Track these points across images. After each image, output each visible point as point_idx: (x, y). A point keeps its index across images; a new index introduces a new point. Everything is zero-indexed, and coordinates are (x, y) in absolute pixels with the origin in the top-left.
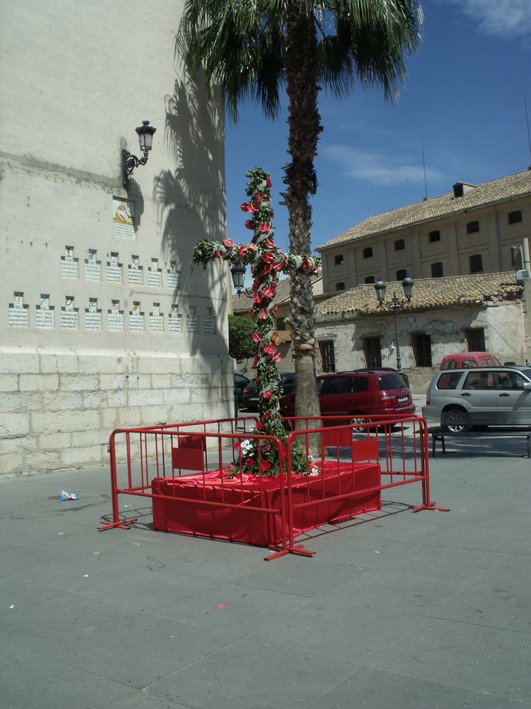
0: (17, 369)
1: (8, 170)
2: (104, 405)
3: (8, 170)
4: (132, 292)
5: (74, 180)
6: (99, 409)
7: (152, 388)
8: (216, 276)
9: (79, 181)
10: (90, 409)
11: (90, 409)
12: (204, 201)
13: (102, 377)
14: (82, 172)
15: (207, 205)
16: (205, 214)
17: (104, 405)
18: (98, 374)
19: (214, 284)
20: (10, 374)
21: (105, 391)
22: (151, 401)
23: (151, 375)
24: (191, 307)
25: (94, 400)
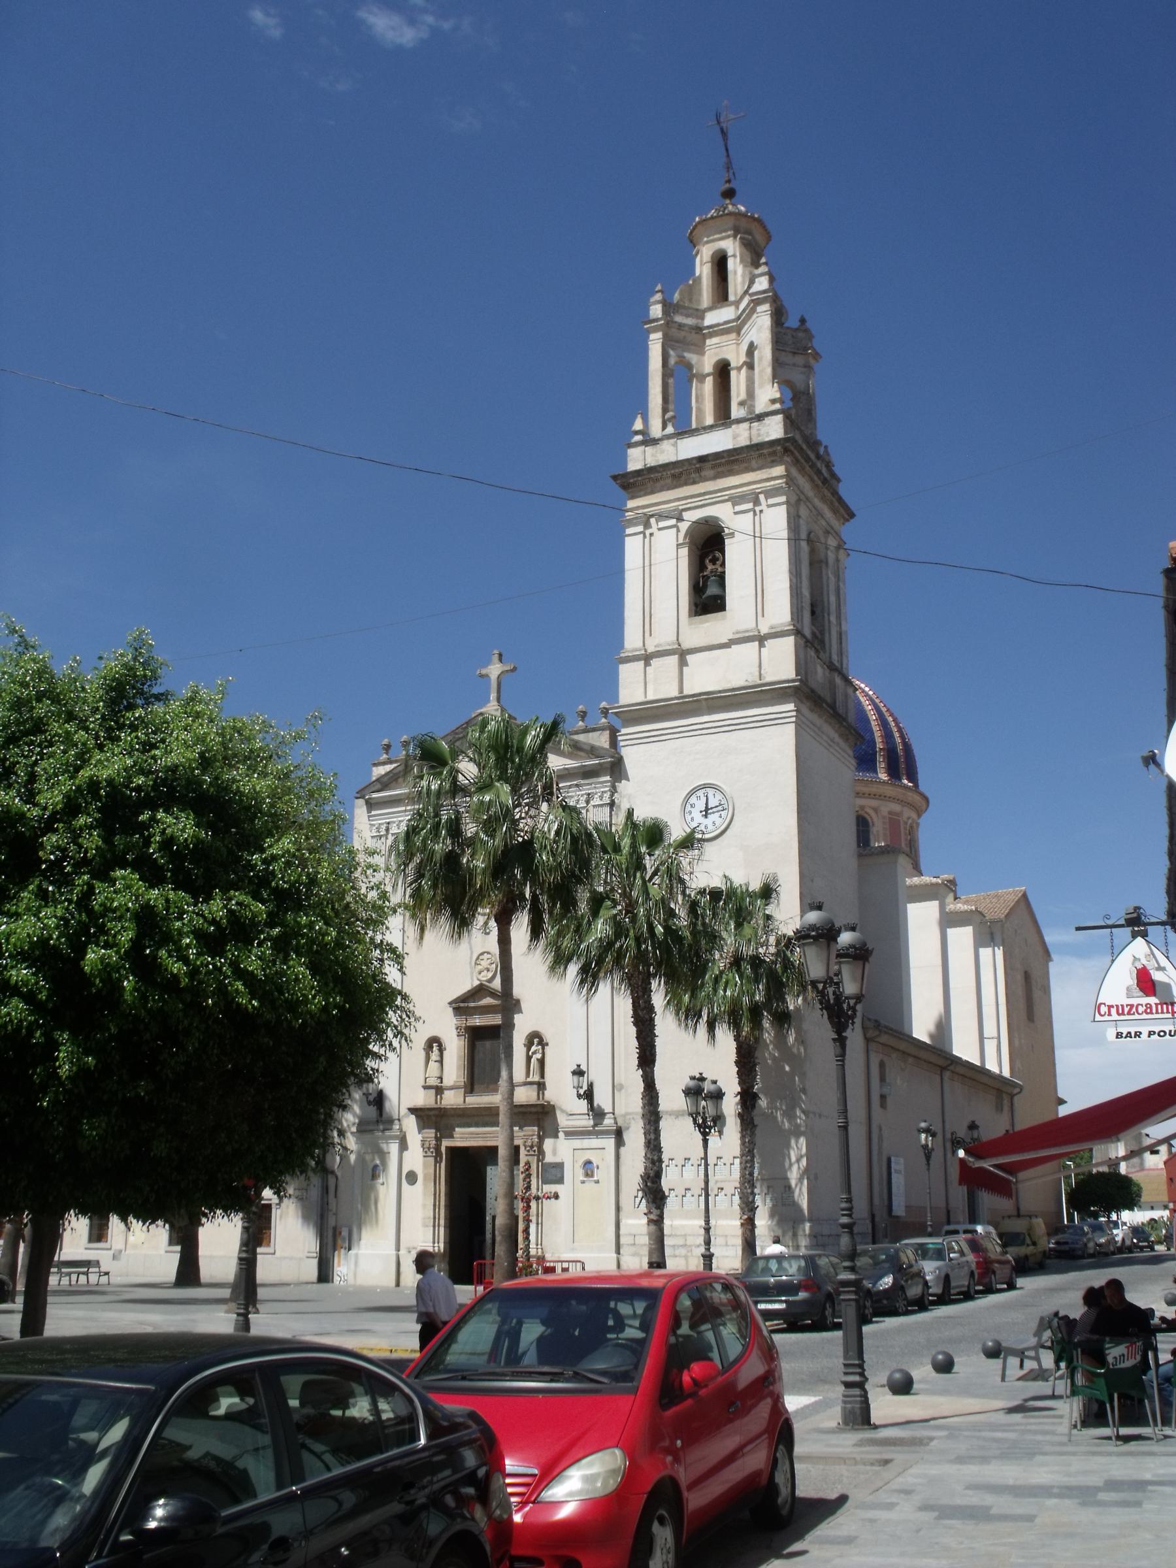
0: (634, 1232)
1: (633, 1122)
2: (689, 1254)
3: (633, 1122)
4: (716, 1182)
5: (673, 1117)
6: (686, 1257)
7: (727, 1245)
8: (793, 1159)
9: (677, 1117)
10: (680, 1256)
11: (680, 1256)
12: (781, 1105)
13: (688, 1238)
14: (679, 1111)
15: (784, 1108)
16: (783, 1115)
17: (689, 1254)
18: (685, 1235)
19: (791, 1165)
20: (630, 1235)
21: (690, 1246)
22: (727, 1254)
23: (726, 1236)
24: (769, 1187)
25: (683, 1251)
